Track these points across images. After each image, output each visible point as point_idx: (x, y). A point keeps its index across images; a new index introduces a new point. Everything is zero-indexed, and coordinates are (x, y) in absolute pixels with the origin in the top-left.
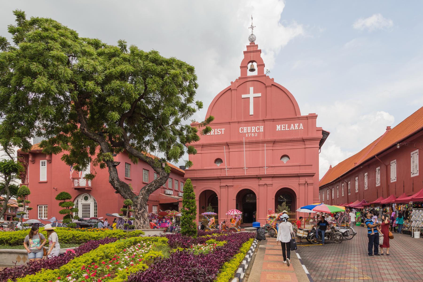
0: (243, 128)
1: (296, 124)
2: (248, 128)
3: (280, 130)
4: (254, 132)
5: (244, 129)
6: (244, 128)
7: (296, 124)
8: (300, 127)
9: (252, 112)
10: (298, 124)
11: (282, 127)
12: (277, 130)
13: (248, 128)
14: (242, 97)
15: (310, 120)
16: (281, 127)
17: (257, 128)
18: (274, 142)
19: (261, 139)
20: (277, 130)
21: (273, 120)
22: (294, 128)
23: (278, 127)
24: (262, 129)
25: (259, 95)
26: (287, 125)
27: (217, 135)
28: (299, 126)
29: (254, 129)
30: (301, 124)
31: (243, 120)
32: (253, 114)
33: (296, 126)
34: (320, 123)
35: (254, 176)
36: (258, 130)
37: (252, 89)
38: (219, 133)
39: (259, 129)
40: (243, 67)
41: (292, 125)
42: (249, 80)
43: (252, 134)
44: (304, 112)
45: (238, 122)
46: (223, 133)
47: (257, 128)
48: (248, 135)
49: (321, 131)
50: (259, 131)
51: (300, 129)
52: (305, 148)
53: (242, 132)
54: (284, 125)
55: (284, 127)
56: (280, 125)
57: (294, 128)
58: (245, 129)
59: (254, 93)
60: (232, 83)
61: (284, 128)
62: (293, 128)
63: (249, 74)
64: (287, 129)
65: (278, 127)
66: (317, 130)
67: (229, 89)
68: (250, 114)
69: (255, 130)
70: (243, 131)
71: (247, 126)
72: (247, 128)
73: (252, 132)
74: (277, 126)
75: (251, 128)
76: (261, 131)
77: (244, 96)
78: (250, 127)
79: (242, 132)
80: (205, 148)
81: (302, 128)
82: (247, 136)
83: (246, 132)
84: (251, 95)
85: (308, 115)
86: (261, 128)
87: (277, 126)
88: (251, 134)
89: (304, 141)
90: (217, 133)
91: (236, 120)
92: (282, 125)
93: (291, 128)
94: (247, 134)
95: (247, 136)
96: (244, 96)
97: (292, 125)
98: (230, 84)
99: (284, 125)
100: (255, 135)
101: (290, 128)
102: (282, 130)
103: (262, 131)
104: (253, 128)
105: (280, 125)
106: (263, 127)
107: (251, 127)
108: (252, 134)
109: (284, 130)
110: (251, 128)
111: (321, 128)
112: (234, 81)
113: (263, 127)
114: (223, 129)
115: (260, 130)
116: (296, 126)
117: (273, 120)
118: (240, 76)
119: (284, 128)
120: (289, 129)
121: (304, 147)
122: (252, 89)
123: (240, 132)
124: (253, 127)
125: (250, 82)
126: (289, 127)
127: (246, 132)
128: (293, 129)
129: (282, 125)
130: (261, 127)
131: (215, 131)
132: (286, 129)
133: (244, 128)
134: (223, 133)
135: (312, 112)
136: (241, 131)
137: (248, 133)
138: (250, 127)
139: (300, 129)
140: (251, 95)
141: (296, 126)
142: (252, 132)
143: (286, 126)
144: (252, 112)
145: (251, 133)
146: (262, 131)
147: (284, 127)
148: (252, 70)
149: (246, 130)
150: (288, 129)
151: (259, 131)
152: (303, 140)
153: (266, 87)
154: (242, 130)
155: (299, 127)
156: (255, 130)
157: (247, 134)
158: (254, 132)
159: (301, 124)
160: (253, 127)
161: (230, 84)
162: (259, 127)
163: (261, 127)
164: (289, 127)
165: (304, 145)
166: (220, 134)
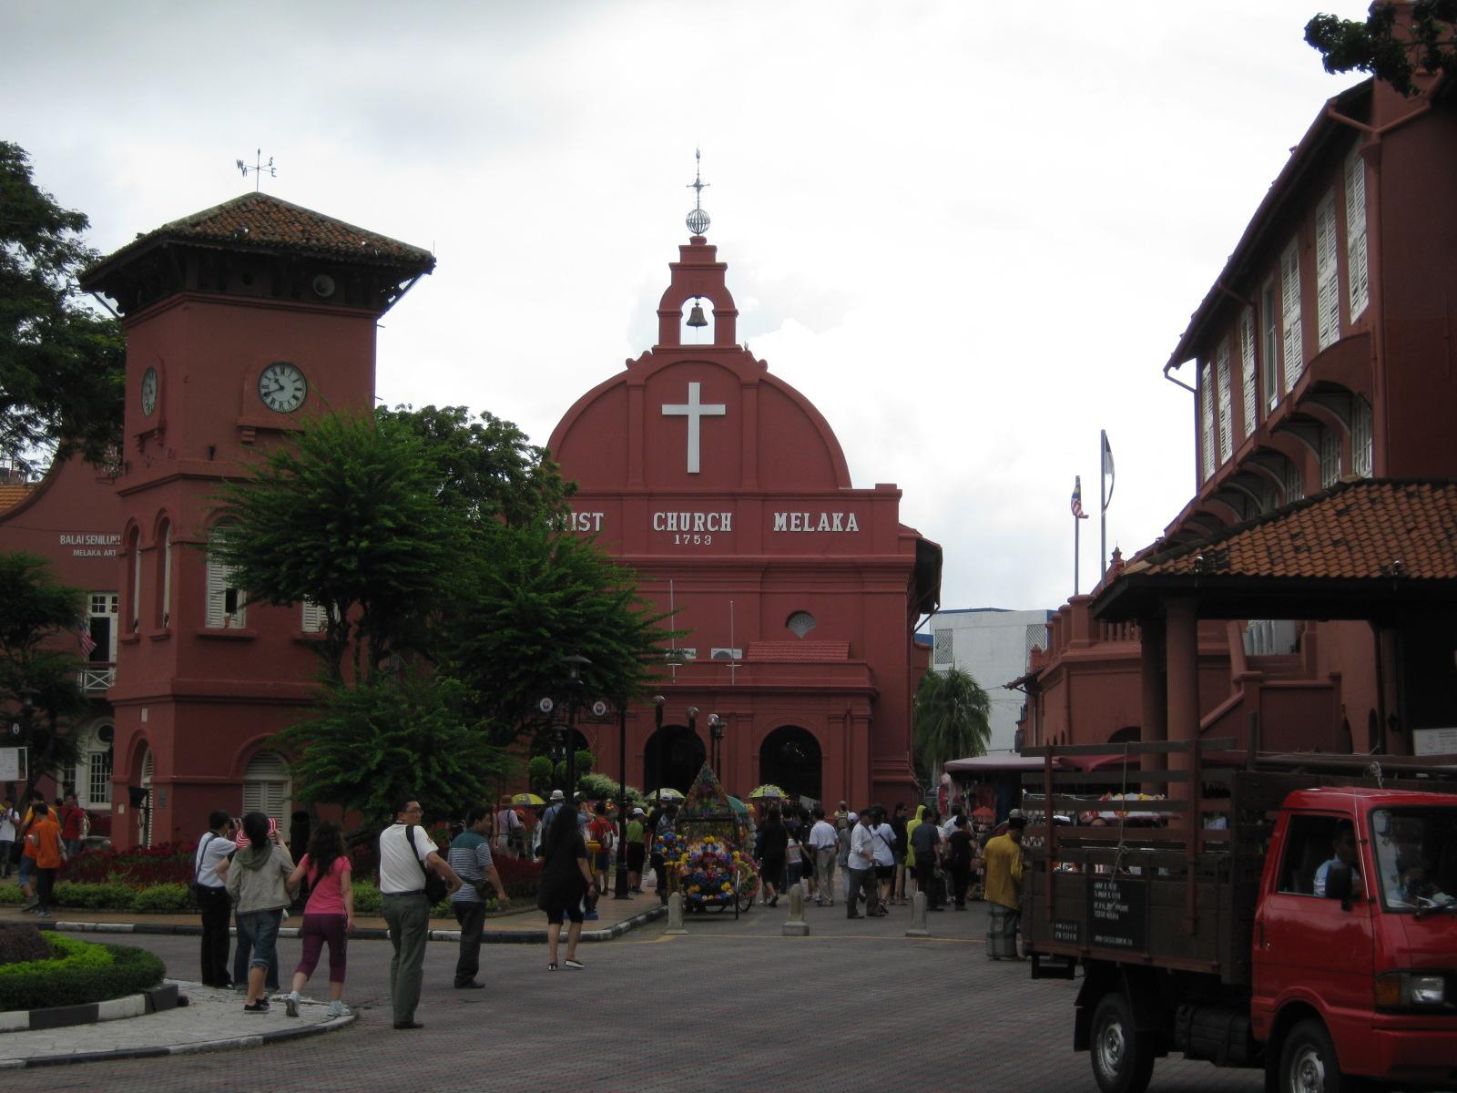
1: (835, 515)
2: (682, 515)
3: (784, 529)
4: (702, 529)
6: (669, 514)
7: (835, 515)
8: (849, 525)
9: (693, 465)
10: (841, 515)
11: (793, 522)
12: (776, 529)
13: (682, 515)
14: (664, 413)
16: (789, 520)
18: (767, 569)
20: (776, 529)
22: (831, 525)
24: (726, 523)
25: (719, 409)
26: (807, 515)
28: (844, 522)
29: (699, 521)
30: (852, 516)
33: (832, 522)
34: (911, 515)
36: (713, 526)
37: (694, 389)
39: (716, 522)
40: (669, 315)
41: (824, 516)
43: (696, 537)
44: (863, 477)
45: (651, 495)
46: (598, 529)
48: (682, 540)
49: (914, 543)
50: (717, 528)
51: (848, 529)
52: (863, 593)
54: (800, 515)
56: (785, 515)
57: (831, 525)
58: (672, 519)
59: (704, 399)
60: (629, 362)
61: (796, 526)
62: (827, 525)
63: (691, 336)
64: (806, 529)
65: (780, 521)
66: (901, 539)
68: (689, 471)
69: (705, 524)
70: (666, 526)
72: (679, 518)
73: (696, 529)
74: (777, 515)
75: (692, 519)
76: (723, 529)
77: (668, 409)
78: (688, 515)
79: (663, 527)
81: (856, 529)
82: (678, 542)
83: (675, 529)
84: (694, 408)
85: (873, 487)
86: (723, 518)
87: (777, 515)
88: (691, 540)
93: (821, 525)
94: (677, 537)
95: (678, 542)
96: (668, 409)
97: (824, 516)
98: (626, 368)
99: (800, 515)
100: (703, 540)
102: (793, 529)
103: (729, 529)
104: (697, 518)
105: (785, 515)
106: (729, 515)
108: (696, 537)
109: (799, 529)
110: (692, 519)
111: (914, 531)
112: (635, 358)
114: (598, 515)
116: (837, 522)
117: (765, 497)
118: (657, 344)
119: (796, 526)
120: (813, 529)
122: (694, 389)
124: (697, 515)
126: (814, 521)
127: (675, 529)
128: (827, 529)
132: (802, 525)
134: (598, 529)
135: (886, 480)
137: (680, 532)
138: (688, 515)
139: (848, 529)
140: (694, 408)
141: (837, 522)
142: (696, 529)
143: (802, 519)
144: (693, 465)
145: (691, 532)
146: (729, 529)
147: (798, 522)
148: (697, 320)
150: (810, 526)
151: (717, 528)
152: (858, 569)
154: (662, 521)
156: (705, 524)
157: (677, 537)
158: (702, 529)
159: (852, 516)
160: (697, 515)
161: (626, 368)
163: (723, 515)
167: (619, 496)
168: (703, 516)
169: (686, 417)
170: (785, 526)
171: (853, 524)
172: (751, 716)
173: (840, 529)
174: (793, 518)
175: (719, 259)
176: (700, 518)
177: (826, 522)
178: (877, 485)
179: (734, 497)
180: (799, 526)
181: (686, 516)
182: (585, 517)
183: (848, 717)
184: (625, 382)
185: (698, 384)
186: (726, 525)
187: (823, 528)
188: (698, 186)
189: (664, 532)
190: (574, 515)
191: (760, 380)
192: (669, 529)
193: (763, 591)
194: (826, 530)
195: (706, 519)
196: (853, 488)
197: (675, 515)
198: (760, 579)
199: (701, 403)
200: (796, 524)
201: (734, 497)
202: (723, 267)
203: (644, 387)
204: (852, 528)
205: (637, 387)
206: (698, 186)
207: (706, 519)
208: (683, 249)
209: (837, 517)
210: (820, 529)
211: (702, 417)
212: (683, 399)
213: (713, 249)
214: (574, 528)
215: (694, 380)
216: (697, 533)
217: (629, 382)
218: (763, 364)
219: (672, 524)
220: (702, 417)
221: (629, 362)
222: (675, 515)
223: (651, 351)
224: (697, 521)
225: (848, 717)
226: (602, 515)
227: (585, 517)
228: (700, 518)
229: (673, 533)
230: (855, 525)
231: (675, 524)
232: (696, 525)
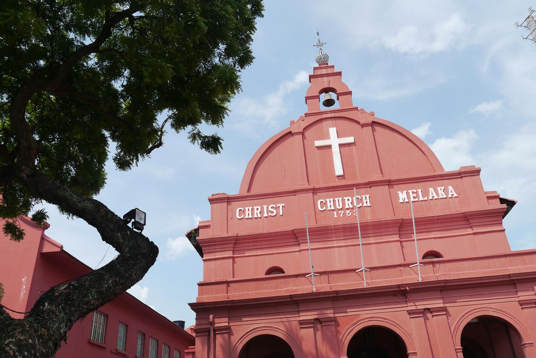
1: (439, 188)
2: (336, 199)
3: (407, 200)
6: (328, 200)
7: (439, 188)
8: (450, 193)
9: (339, 170)
11: (412, 195)
13: (336, 199)
15: (467, 180)
17: (354, 198)
19: (369, 218)
20: (401, 201)
21: (390, 183)
22: (438, 195)
23: (402, 196)
24: (366, 201)
26: (420, 191)
28: (446, 191)
30: (450, 188)
31: (322, 185)
32: (342, 174)
35: (391, 287)
36: (358, 203)
37: (333, 131)
38: (273, 212)
39: (360, 201)
41: (431, 190)
42: (325, 116)
46: (281, 214)
47: (354, 198)
48: (338, 214)
49: (498, 200)
53: (325, 208)
55: (415, 195)
56: (405, 192)
57: (438, 195)
62: (434, 194)
64: (421, 198)
65: (402, 196)
66: (489, 198)
67: (289, 134)
71: (334, 197)
73: (347, 207)
74: (400, 193)
75: (343, 200)
76: (365, 205)
77: (318, 143)
78: (340, 199)
80: (241, 245)
81: (455, 195)
82: (336, 216)
86: (364, 198)
87: (400, 193)
89: (468, 220)
91: (307, 186)
92: (410, 192)
95: (336, 216)
97: (431, 190)
99: (415, 191)
100: (353, 213)
101: (428, 195)
103: (369, 204)
105: (405, 192)
106: (368, 196)
107: (343, 196)
108: (347, 212)
109: (417, 199)
110: (343, 200)
111: (496, 192)
114: (281, 205)
115: (363, 204)
117: (390, 183)
120: (426, 199)
121: (470, 231)
122: (333, 131)
124: (346, 198)
125: (330, 122)
126: (425, 193)
127: (333, 208)
128: (436, 197)
129: (410, 192)
130: (364, 197)
132: (417, 196)
133: (328, 200)
139: (450, 196)
144: (339, 170)
149: (332, 204)
151: (361, 205)
153: (363, 126)
154: (323, 204)
155: (447, 194)
157: (335, 213)
158: (351, 206)
159: (450, 188)
160: (346, 198)
162: (360, 197)
163: (364, 197)
164: (425, 193)
165: (471, 229)
167: (295, 192)
168: (350, 198)
169: (330, 147)
171: (452, 191)
172: (444, 309)
174: (411, 193)
175: (336, 70)
176: (348, 200)
178: (462, 167)
179: (370, 184)
180: (416, 197)
181: (339, 200)
182: (272, 207)
184: (291, 132)
185: (335, 129)
186: (367, 202)
187: (433, 197)
188: (320, 44)
190: (265, 207)
191: (373, 122)
192: (328, 209)
193: (401, 240)
194: (435, 198)
195: (352, 200)
196: (446, 171)
198: (398, 232)
200: (414, 197)
201: (370, 184)
202: (339, 74)
203: (303, 133)
205: (298, 133)
206: (320, 44)
207: (352, 200)
208: (315, 69)
210: (431, 198)
211: (341, 145)
212: (328, 137)
213: (333, 67)
214: (266, 215)
215: (333, 127)
216: (347, 209)
217: (292, 132)
218: (372, 114)
219: (330, 205)
220: (341, 145)
221: (292, 123)
222: (332, 200)
223: (304, 115)
227: (272, 207)
228: (348, 200)
230: (454, 193)
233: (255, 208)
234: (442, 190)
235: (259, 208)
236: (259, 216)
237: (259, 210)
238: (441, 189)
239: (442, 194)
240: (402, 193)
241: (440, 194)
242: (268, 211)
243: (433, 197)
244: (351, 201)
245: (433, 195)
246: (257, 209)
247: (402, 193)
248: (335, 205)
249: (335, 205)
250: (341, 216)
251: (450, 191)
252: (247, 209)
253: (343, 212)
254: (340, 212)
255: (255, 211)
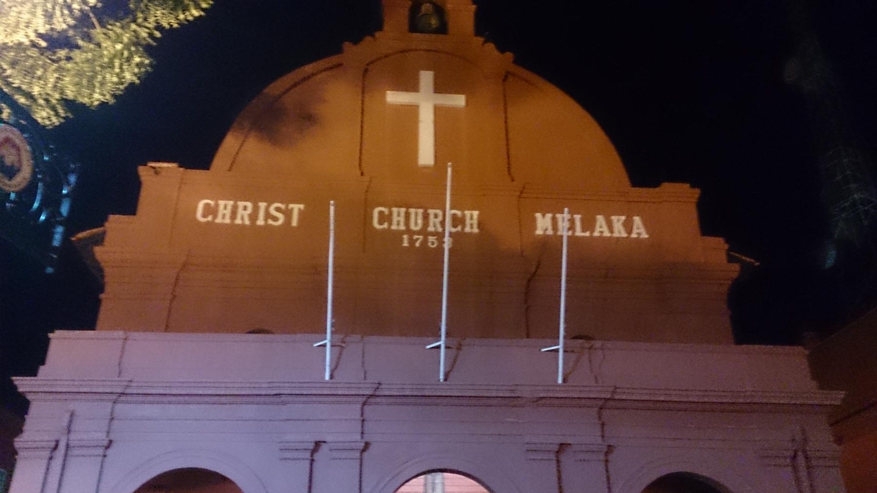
0: (391, 213)
1: (614, 218)
5: (395, 215)
8: (635, 231)
10: (623, 218)
12: (539, 232)
20: (539, 232)
22: (611, 231)
25: (459, 101)
26: (578, 217)
27: (267, 227)
28: (628, 226)
30: (637, 220)
38: (275, 219)
41: (600, 219)
43: (431, 239)
46: (294, 223)
48: (412, 242)
51: (634, 235)
53: (386, 225)
56: (549, 216)
57: (611, 231)
72: (407, 216)
73: (431, 229)
74: (538, 215)
75: (426, 217)
76: (468, 229)
78: (420, 211)
79: (386, 225)
81: (645, 236)
82: (406, 244)
83: (402, 227)
87: (538, 215)
88: (425, 241)
90: (266, 220)
93: (598, 229)
94: (405, 237)
95: (406, 244)
97: (600, 219)
101: (592, 231)
104: (432, 217)
106: (476, 213)
108: (431, 239)
110: (426, 217)
113: (476, 213)
114: (296, 208)
115: (464, 227)
120: (587, 234)
122: (426, 78)
123: (376, 224)
124: (431, 212)
126: (588, 224)
127: (402, 227)
128: (607, 234)
131: (256, 209)
134: (294, 223)
136: (381, 222)
137: (409, 231)
138: (420, 211)
139: (634, 235)
142: (431, 229)
145: (424, 232)
146: (476, 230)
149: (402, 219)
150: (583, 231)
155: (630, 232)
156: (443, 223)
157: (405, 237)
159: (637, 220)
160: (431, 212)
164: (588, 224)
166: (280, 222)
170: (550, 228)
171: (640, 230)
173: (625, 235)
176: (436, 216)
177: (604, 224)
183: (801, 460)
189: (389, 230)
190: (262, 205)
192: (394, 227)
197: (403, 210)
199: (435, 92)
204: (639, 234)
209: (618, 221)
210: (596, 234)
214: (260, 222)
216: (433, 234)
219: (398, 223)
224: (432, 219)
225: (801, 460)
226: (302, 206)
227: (278, 209)
229: (402, 233)
231: (402, 223)
232: (431, 223)
233: (241, 204)
234: (621, 221)
235: (249, 205)
236: (247, 222)
237: (249, 211)
238: (618, 220)
239: (619, 231)
240: (544, 216)
241: (616, 230)
242: (268, 215)
243: (602, 232)
244: (440, 218)
245: (601, 230)
246: (245, 208)
247: (544, 216)
248: (407, 223)
249: (407, 223)
250: (417, 244)
251: (635, 227)
252: (222, 203)
253: (421, 237)
254: (415, 237)
255: (240, 211)
